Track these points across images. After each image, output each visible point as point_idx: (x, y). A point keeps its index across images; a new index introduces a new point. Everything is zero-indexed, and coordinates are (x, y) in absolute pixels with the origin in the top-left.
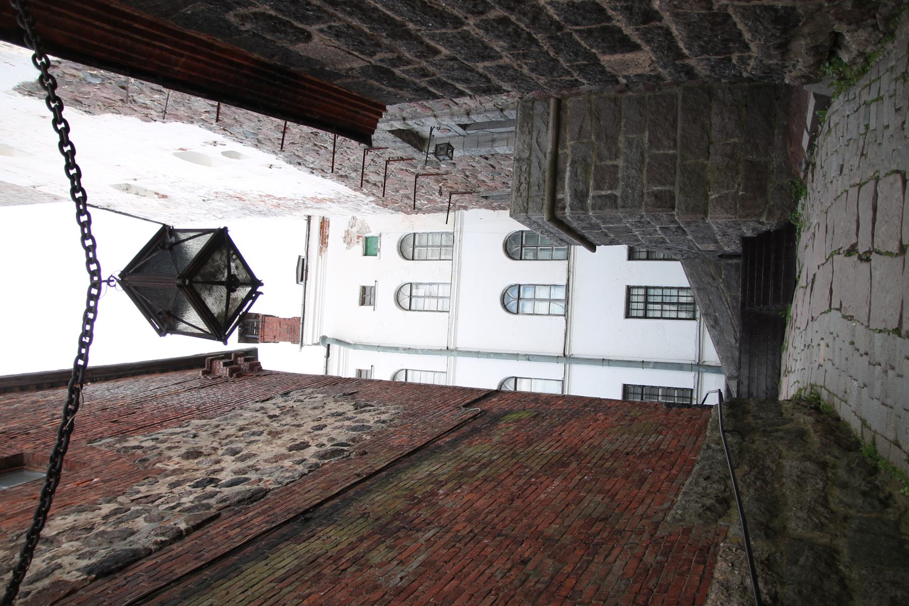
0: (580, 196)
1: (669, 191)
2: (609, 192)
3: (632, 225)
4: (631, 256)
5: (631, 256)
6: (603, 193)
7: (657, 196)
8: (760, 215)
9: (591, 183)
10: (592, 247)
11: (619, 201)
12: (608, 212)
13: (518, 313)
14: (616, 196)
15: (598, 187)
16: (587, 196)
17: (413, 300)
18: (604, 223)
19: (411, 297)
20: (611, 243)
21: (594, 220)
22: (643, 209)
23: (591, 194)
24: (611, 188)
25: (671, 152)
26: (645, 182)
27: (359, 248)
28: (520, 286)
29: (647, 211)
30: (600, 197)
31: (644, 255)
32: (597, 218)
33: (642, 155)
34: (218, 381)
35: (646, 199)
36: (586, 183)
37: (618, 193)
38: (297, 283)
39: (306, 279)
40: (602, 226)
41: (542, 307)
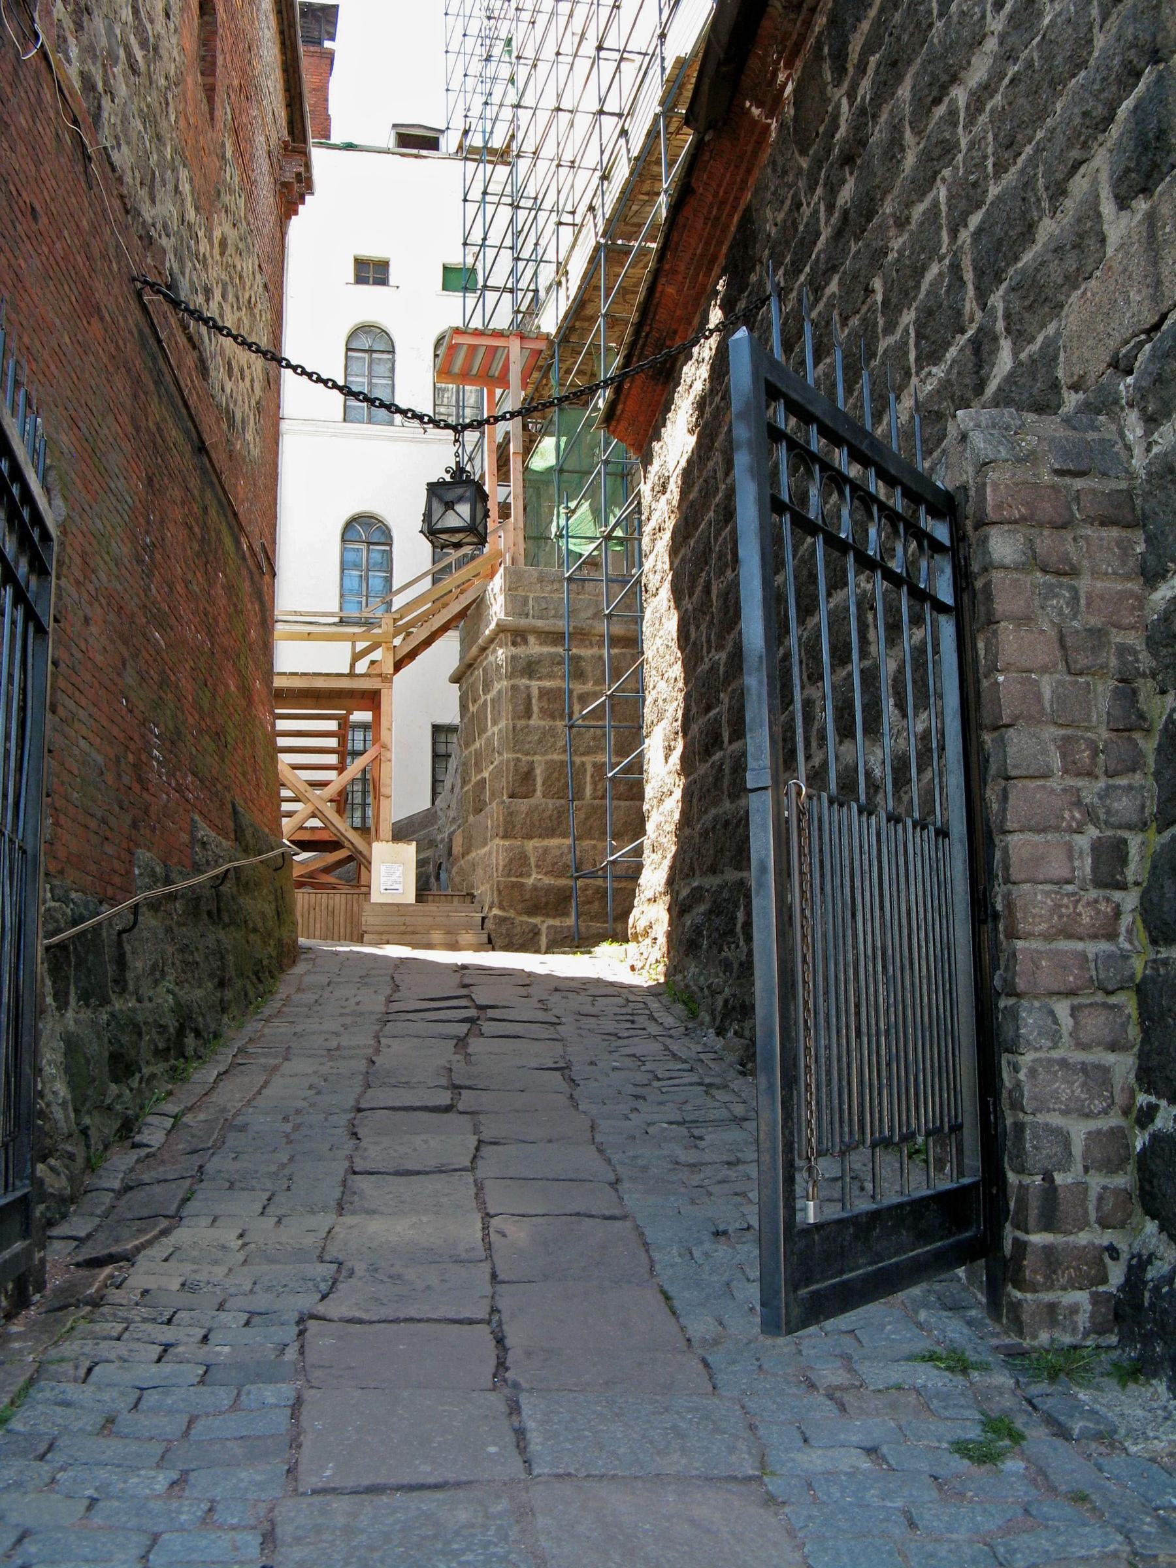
0: (529, 668)
1: (534, 791)
2: (535, 709)
3: (488, 739)
4: (437, 729)
5: (437, 729)
6: (534, 701)
7: (527, 776)
8: (501, 907)
9: (548, 684)
10: (457, 679)
11: (523, 722)
12: (506, 708)
13: (343, 540)
14: (529, 718)
15: (543, 693)
16: (530, 678)
17: (366, 355)
18: (493, 700)
19: (370, 351)
20: (464, 707)
21: (497, 686)
22: (511, 756)
23: (535, 685)
24: (541, 709)
25: (588, 791)
26: (549, 757)
27: (455, 258)
28: (390, 545)
29: (508, 761)
30: (529, 697)
31: (442, 750)
32: (500, 692)
33: (583, 754)
34: (276, 167)
35: (524, 758)
36: (550, 676)
37: (535, 721)
38: (395, 126)
39: (402, 155)
40: (489, 697)
41: (353, 581)
